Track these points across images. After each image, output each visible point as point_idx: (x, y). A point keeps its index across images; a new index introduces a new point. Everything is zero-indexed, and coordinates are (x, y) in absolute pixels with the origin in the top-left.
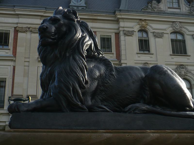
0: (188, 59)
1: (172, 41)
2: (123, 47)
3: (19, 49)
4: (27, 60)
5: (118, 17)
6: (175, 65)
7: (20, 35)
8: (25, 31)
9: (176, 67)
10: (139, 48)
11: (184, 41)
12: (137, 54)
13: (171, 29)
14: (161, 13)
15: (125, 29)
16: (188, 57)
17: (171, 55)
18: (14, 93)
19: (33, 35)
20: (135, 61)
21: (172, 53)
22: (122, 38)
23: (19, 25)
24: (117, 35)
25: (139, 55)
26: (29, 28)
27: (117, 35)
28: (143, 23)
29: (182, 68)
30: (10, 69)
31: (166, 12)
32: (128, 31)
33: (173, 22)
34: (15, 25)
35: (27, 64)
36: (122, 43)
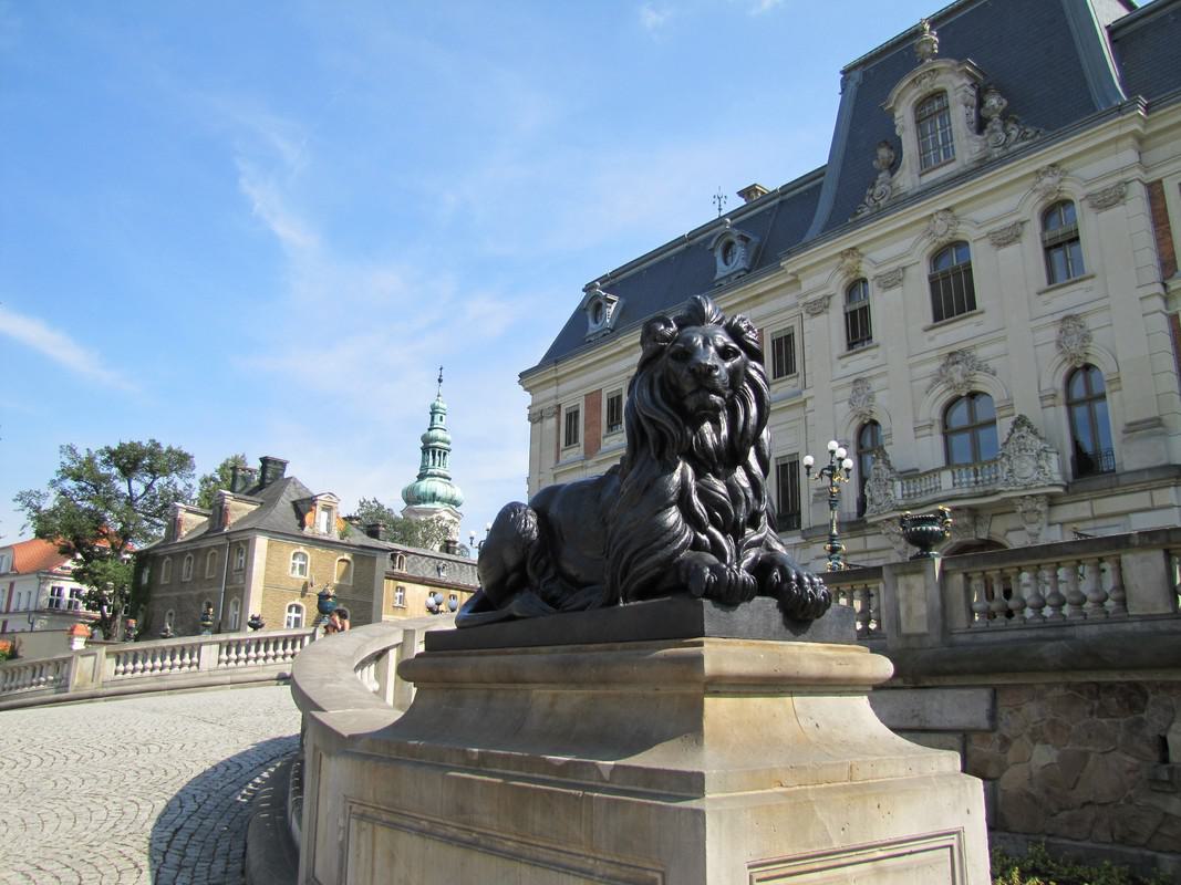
0: (978, 324)
5: (789, 271)
6: (939, 357)
9: (943, 362)
10: (848, 339)
11: (968, 270)
12: (840, 358)
13: (926, 242)
14: (901, 202)
15: (811, 298)
20: (834, 384)
28: (849, 261)
29: (953, 364)
31: (910, 194)
32: (815, 302)
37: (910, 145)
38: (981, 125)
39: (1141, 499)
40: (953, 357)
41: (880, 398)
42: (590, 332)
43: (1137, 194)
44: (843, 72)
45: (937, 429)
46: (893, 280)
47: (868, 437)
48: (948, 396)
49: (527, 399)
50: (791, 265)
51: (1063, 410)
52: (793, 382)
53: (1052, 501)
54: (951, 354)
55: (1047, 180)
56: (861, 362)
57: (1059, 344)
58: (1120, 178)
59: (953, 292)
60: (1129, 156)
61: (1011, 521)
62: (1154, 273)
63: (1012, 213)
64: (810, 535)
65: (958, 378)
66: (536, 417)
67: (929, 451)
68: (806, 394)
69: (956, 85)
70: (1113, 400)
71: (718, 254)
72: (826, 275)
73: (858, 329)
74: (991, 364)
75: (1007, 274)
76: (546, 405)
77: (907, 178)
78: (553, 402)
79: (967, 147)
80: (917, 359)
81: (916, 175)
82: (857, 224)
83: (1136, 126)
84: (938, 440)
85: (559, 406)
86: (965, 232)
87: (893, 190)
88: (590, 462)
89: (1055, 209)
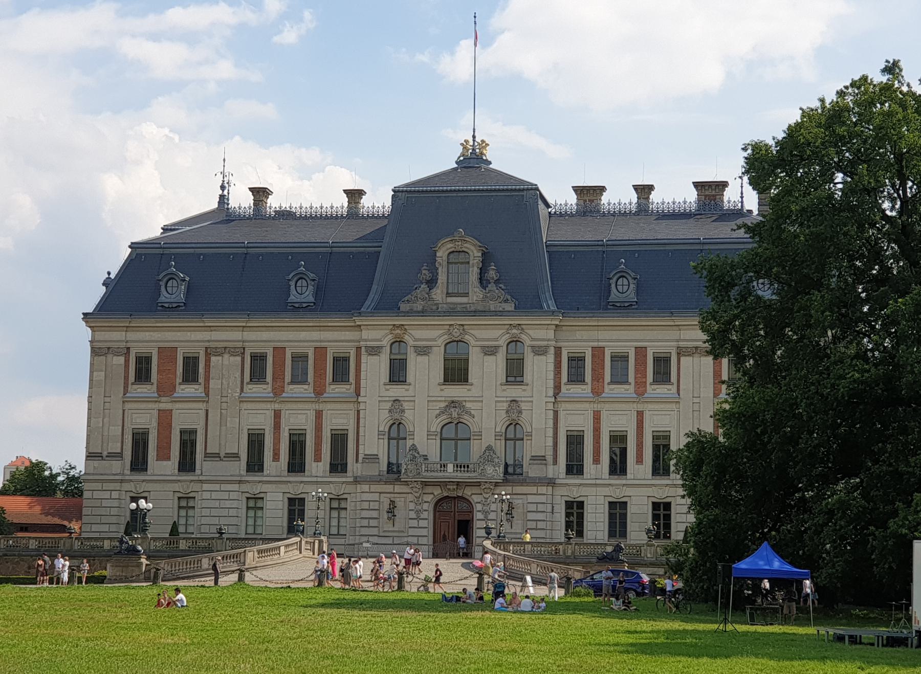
0: (469, 390)
2: (363, 376)
3: (212, 383)
4: (224, 399)
7: (213, 359)
8: (220, 352)
16: (468, 387)
18: (208, 451)
19: (232, 358)
22: (364, 358)
23: (212, 345)
24: (359, 349)
25: (388, 387)
26: (225, 348)
27: (359, 349)
30: (203, 413)
32: (373, 347)
34: (207, 344)
35: (224, 405)
36: (363, 366)
37: (442, 278)
38: (483, 281)
39: (533, 489)
40: (453, 404)
41: (408, 414)
42: (162, 299)
43: (552, 351)
44: (393, 191)
45: (438, 438)
46: (423, 351)
47: (396, 432)
49: (86, 333)
52: (348, 387)
53: (497, 484)
55: (514, 331)
56: (397, 391)
57: (507, 412)
58: (545, 343)
59: (456, 372)
60: (551, 334)
61: (476, 490)
62: (551, 393)
63: (496, 340)
64: (357, 481)
65: (455, 415)
66: (96, 351)
67: (431, 449)
68: (360, 399)
70: (527, 443)
71: (292, 283)
72: (383, 333)
73: (397, 373)
74: (473, 412)
75: (487, 370)
76: (116, 345)
77: (438, 294)
78: (123, 345)
79: (476, 294)
80: (433, 399)
81: (444, 296)
82: (410, 313)
83: (557, 323)
85: (128, 348)
87: (431, 299)
88: (163, 399)
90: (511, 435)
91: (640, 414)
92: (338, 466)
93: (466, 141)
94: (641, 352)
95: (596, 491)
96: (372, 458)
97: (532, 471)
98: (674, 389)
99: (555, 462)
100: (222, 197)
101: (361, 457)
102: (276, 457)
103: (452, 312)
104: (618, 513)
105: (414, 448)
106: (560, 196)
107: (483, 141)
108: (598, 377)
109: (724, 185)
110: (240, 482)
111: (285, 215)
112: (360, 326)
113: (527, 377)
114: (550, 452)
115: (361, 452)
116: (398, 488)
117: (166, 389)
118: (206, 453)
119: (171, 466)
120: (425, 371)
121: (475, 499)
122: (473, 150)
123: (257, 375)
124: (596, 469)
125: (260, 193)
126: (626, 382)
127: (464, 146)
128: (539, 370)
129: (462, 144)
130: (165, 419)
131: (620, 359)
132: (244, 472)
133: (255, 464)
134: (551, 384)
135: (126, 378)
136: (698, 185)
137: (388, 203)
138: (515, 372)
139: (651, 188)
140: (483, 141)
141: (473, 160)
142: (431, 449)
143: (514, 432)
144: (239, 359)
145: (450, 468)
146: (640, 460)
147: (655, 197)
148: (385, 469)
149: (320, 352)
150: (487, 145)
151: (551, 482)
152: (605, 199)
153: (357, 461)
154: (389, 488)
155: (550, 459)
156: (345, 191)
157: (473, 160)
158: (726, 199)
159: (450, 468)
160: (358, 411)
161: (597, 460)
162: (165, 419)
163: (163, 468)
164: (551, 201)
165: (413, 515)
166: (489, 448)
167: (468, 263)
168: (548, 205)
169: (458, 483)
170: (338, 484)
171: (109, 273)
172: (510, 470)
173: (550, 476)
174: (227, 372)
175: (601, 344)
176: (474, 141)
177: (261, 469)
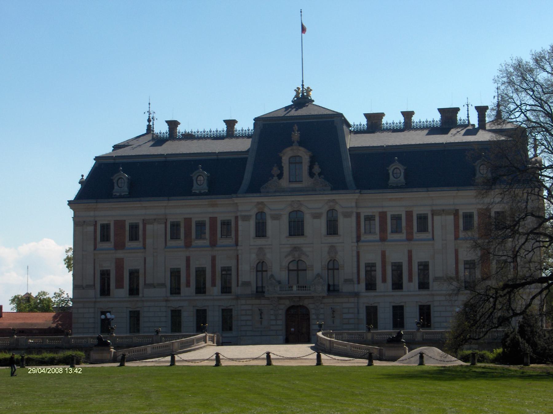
1: (290, 222)
3: (149, 241)
7: (148, 227)
11: (302, 222)
15: (243, 214)
17: (287, 237)
18: (147, 282)
21: (288, 234)
22: (240, 223)
24: (237, 218)
27: (237, 218)
33: (293, 201)
36: (240, 228)
38: (311, 175)
40: (296, 249)
44: (254, 120)
46: (276, 217)
47: (261, 268)
48: (292, 259)
49: (71, 213)
50: (237, 200)
51: (326, 271)
53: (323, 297)
54: (295, 248)
55: (331, 204)
56: (261, 242)
60: (354, 204)
62: (355, 240)
64: (238, 298)
67: (283, 276)
68: (239, 248)
69: (305, 155)
73: (261, 231)
77: (284, 183)
79: (307, 181)
84: (287, 272)
85: (96, 222)
86: (303, 209)
89: (332, 211)
90: (331, 266)
91: (410, 252)
92: (226, 289)
93: (298, 88)
94: (409, 214)
95: (384, 298)
96: (246, 284)
97: (345, 288)
98: (430, 236)
99: (359, 282)
100: (149, 127)
101: (240, 283)
102: (188, 284)
103: (293, 192)
104: (398, 313)
105: (272, 276)
106: (356, 118)
107: (308, 88)
108: (383, 229)
109: (457, 110)
110: (167, 301)
111: (188, 136)
112: (236, 203)
113: (341, 230)
114: (355, 277)
115: (240, 280)
116: (263, 302)
117: (119, 246)
118: (145, 284)
119: (124, 292)
120: (277, 228)
121: (310, 307)
122: (303, 94)
123: (175, 236)
124: (384, 287)
125: (172, 125)
126: (401, 232)
127: (297, 91)
128: (346, 225)
129: (295, 90)
130: (119, 264)
131: (397, 218)
132: (169, 294)
133: (176, 290)
134: (354, 235)
135: (95, 239)
136: (440, 110)
137: (252, 127)
138: (332, 229)
139: (412, 113)
140: (308, 88)
141: (302, 99)
142: (283, 276)
143: (333, 266)
144: (163, 226)
145: (295, 288)
146: (410, 280)
147: (415, 119)
148: (255, 289)
149: (213, 220)
150: (311, 90)
151: (356, 295)
152: (384, 121)
153: (238, 286)
154: (257, 301)
155: (355, 280)
156: (225, 121)
157: (302, 99)
158: (458, 118)
159: (295, 288)
160: (238, 256)
161: (384, 280)
162: (119, 264)
163: (120, 293)
164: (351, 123)
165: (273, 317)
166: (318, 275)
167: (301, 163)
168: (349, 125)
169: (300, 297)
170: (226, 301)
171: (82, 176)
172: (331, 288)
173: (356, 290)
174: (155, 232)
175: (385, 210)
176: (303, 88)
177: (179, 293)
